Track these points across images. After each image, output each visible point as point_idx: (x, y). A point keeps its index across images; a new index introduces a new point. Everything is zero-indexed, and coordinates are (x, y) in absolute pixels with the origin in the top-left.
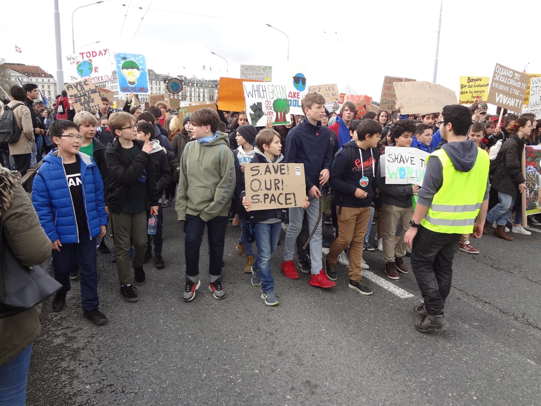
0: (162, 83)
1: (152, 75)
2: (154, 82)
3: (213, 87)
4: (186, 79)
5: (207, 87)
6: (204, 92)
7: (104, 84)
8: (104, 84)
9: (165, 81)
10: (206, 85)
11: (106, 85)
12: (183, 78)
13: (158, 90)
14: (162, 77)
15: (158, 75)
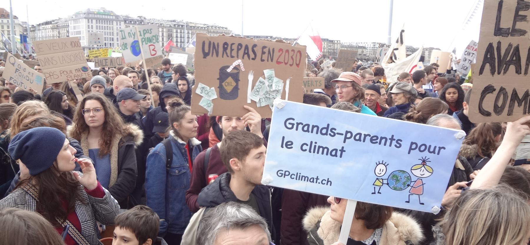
0: (122, 23)
1: (112, 16)
2: (115, 23)
3: (171, 27)
5: (166, 27)
6: (163, 31)
7: (67, 24)
8: (67, 24)
9: (125, 21)
11: (69, 26)
12: (143, 18)
14: (123, 17)
15: (118, 16)
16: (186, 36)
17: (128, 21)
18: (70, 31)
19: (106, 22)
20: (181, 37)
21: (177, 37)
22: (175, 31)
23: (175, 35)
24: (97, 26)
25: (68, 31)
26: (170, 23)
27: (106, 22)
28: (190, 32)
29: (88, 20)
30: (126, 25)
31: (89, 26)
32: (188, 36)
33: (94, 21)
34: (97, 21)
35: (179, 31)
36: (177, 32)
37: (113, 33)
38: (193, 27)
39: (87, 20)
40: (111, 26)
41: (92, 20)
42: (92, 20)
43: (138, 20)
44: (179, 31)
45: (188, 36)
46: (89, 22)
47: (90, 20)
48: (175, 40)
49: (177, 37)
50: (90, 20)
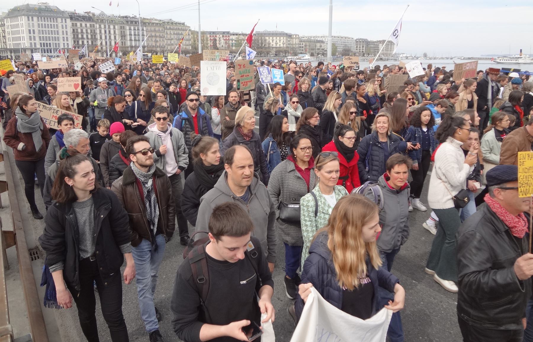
0: (68, 20)
2: (59, 20)
3: (123, 23)
4: (94, 15)
5: (117, 24)
6: (114, 28)
7: (3, 23)
8: (3, 23)
9: (71, 18)
10: (117, 22)
11: (4, 24)
12: (91, 15)
13: (64, 28)
14: (68, 13)
15: (63, 12)
17: (74, 17)
18: (7, 30)
19: (49, 19)
20: (135, 35)
21: (130, 35)
22: (128, 28)
23: (128, 33)
24: (39, 24)
25: (4, 31)
26: (122, 20)
27: (49, 19)
28: (145, 29)
29: (28, 18)
30: (73, 22)
31: (29, 24)
32: (143, 33)
33: (35, 19)
34: (38, 18)
35: (132, 28)
36: (130, 29)
37: (58, 31)
38: (147, 24)
39: (26, 18)
40: (55, 23)
41: (32, 18)
42: (32, 18)
43: (86, 17)
44: (132, 28)
45: (143, 33)
46: (29, 20)
47: (30, 18)
48: (128, 38)
49: (130, 35)
50: (30, 18)
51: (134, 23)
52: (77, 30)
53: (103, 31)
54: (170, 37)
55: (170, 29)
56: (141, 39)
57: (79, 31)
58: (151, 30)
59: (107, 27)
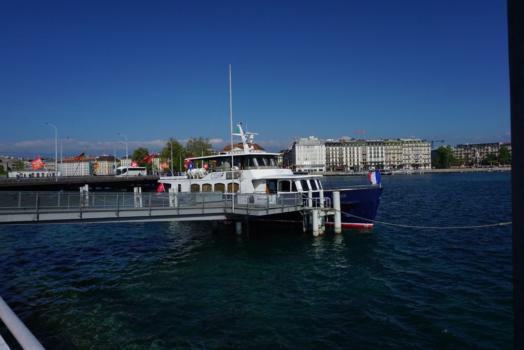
6: (358, 149)
16: (380, 151)
20: (375, 153)
23: (369, 152)
35: (373, 148)
48: (369, 155)
49: (371, 153)
51: (374, 144)
52: (329, 152)
53: (348, 152)
54: (409, 153)
55: (408, 147)
56: (380, 155)
57: (331, 152)
58: (418, 150)
59: (352, 148)
